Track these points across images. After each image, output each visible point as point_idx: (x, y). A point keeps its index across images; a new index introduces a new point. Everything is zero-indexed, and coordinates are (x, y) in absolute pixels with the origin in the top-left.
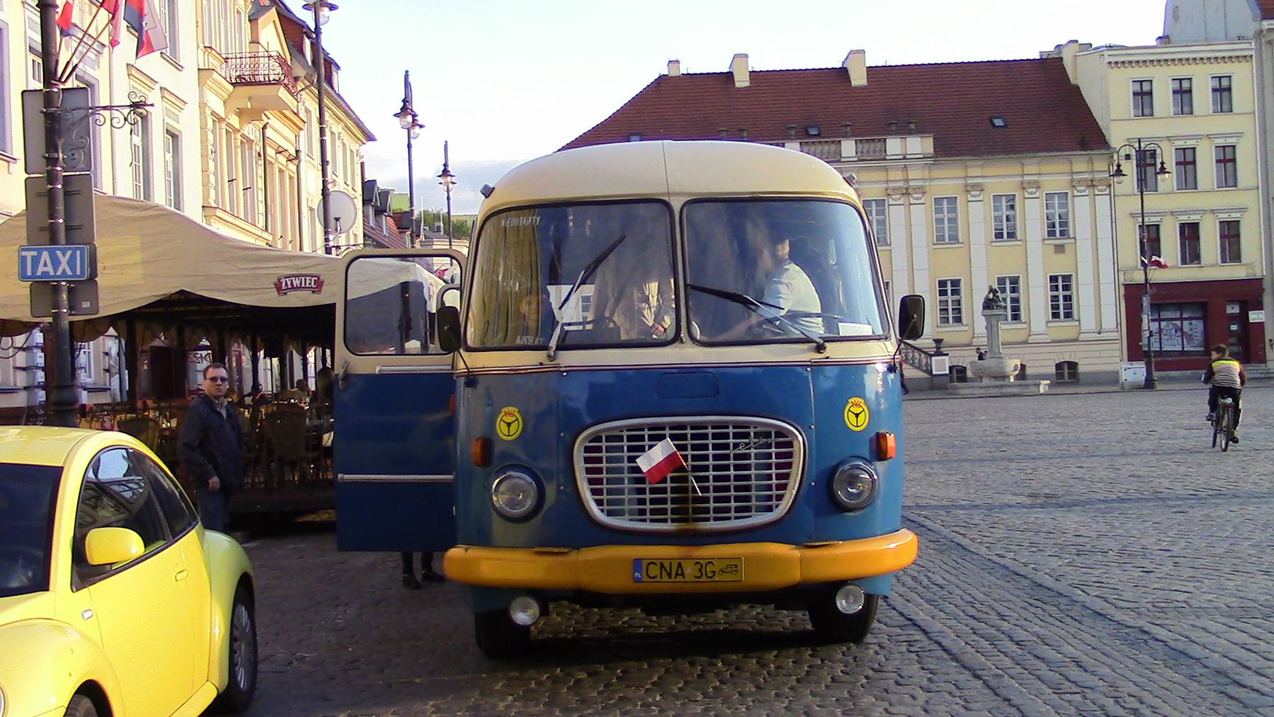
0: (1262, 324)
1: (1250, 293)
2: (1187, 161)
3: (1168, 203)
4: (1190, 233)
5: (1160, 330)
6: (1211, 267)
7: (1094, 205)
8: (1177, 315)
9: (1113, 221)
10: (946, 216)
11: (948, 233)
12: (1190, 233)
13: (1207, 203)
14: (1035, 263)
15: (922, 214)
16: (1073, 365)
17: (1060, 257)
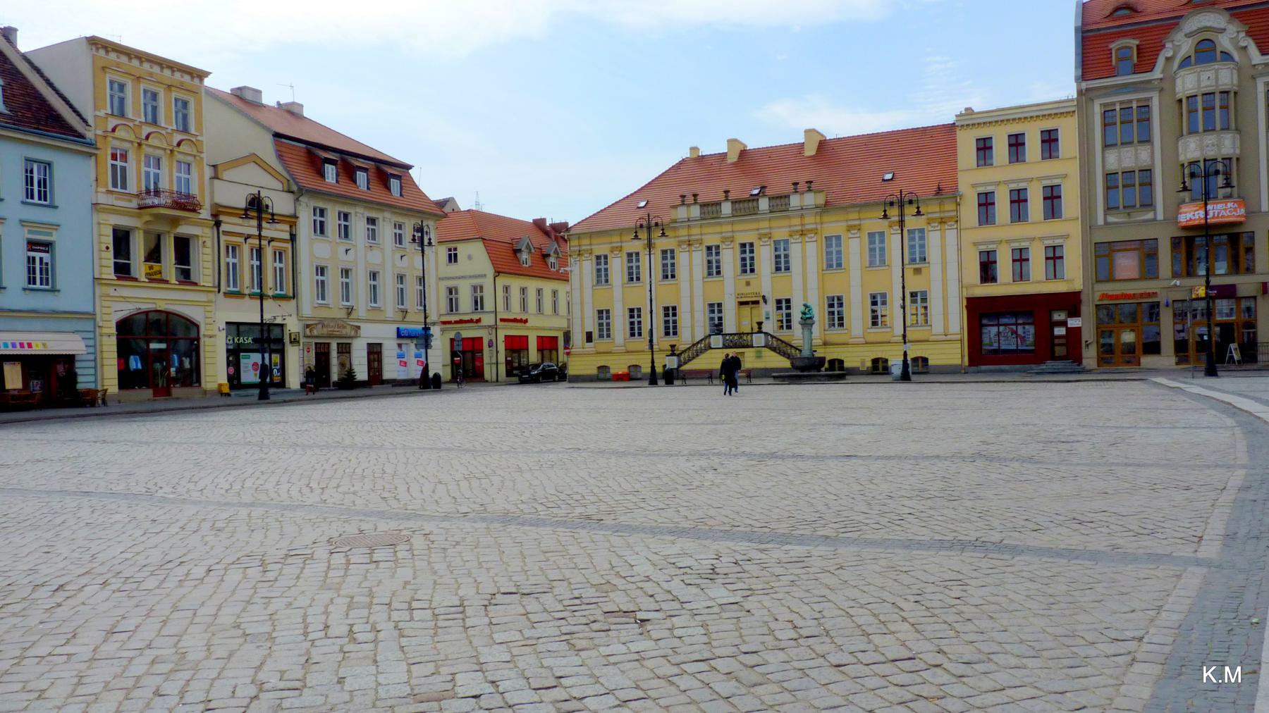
0: (1079, 329)
1: (1071, 303)
2: (1019, 200)
3: (1004, 233)
4: (1020, 258)
5: (999, 334)
6: (1038, 283)
7: (943, 237)
8: (1013, 321)
9: (960, 250)
10: (917, 242)
11: (833, 262)
12: (1020, 258)
15: (699, 257)
16: (925, 360)
17: (918, 277)
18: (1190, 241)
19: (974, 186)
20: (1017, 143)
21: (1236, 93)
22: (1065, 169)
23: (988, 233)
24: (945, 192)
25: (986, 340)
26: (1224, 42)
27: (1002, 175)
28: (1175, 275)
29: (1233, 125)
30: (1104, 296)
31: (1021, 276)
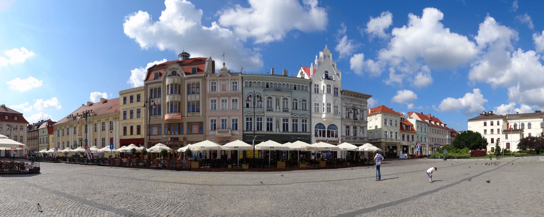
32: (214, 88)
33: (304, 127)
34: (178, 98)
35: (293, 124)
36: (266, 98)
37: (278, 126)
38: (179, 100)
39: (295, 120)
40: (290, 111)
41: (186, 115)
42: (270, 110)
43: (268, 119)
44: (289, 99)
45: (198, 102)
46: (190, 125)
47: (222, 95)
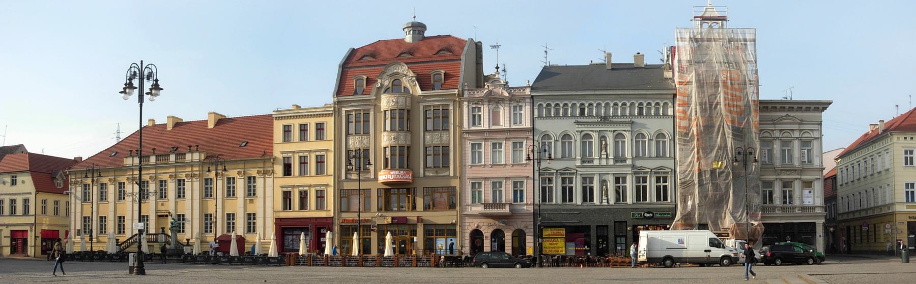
2: (303, 162)
3: (295, 181)
4: (303, 196)
6: (311, 213)
12: (303, 196)
13: (311, 180)
14: (238, 206)
18: (387, 191)
19: (282, 153)
20: (303, 129)
21: (408, 111)
22: (328, 145)
23: (288, 181)
24: (266, 157)
25: (286, 244)
26: (405, 82)
27: (296, 146)
28: (379, 210)
29: (405, 129)
30: (344, 220)
31: (303, 206)
32: (475, 119)
33: (662, 193)
34: (405, 140)
35: (638, 188)
36: (578, 138)
37: (604, 192)
38: (409, 143)
39: (640, 179)
40: (629, 162)
41: (422, 175)
42: (586, 160)
43: (584, 179)
44: (628, 135)
45: (446, 148)
46: (430, 192)
47: (490, 131)
